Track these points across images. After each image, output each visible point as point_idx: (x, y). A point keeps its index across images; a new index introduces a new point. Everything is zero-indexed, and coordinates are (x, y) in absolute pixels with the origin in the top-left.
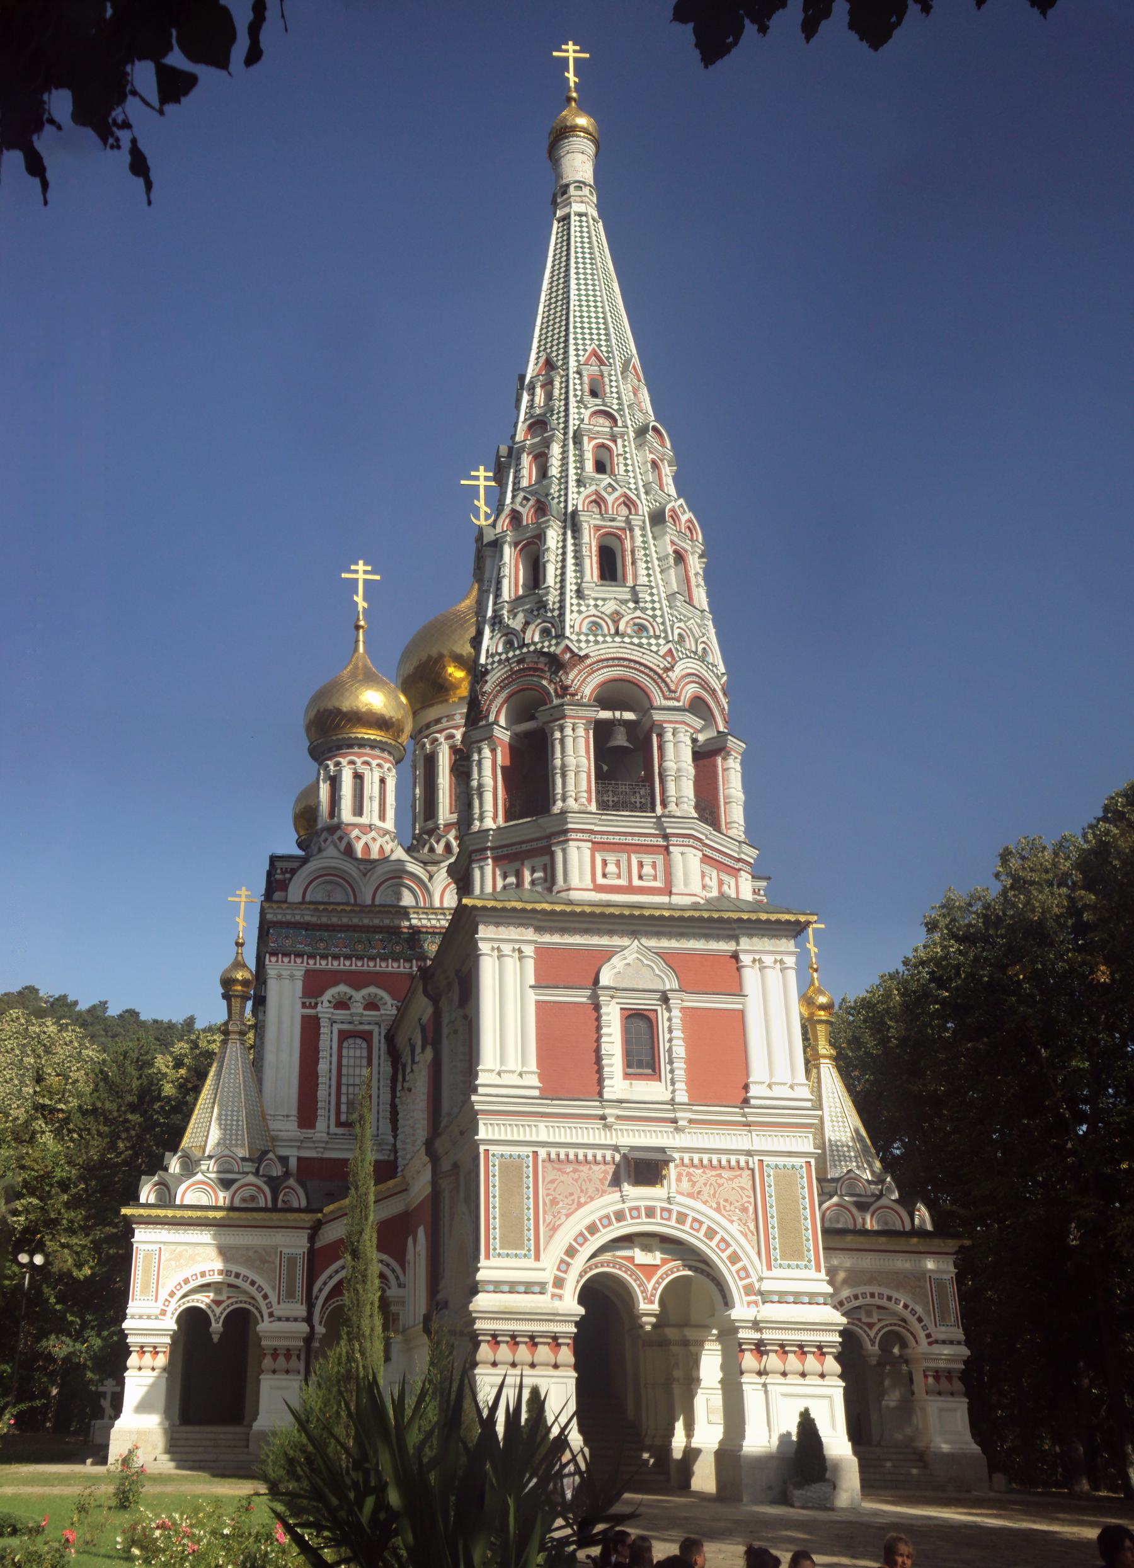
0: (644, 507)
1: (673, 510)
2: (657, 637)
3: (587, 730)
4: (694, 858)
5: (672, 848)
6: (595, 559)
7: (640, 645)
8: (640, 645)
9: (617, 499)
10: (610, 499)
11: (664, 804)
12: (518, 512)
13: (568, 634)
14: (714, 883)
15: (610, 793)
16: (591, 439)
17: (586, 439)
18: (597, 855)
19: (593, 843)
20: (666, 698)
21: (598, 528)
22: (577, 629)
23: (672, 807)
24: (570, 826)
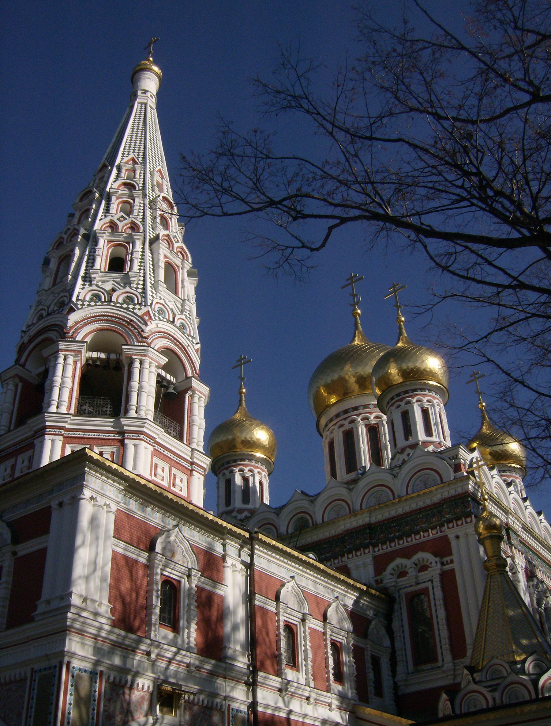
0: (150, 234)
1: (168, 236)
2: (140, 304)
3: (75, 363)
4: (146, 450)
5: (126, 441)
6: (104, 257)
7: (127, 309)
8: (127, 309)
9: (126, 225)
10: (120, 225)
11: (127, 411)
12: (63, 238)
13: (74, 299)
14: (166, 475)
15: (88, 405)
16: (117, 198)
17: (114, 198)
18: (67, 446)
19: (65, 437)
20: (139, 342)
21: (109, 241)
22: (81, 297)
23: (132, 413)
24: (47, 423)
